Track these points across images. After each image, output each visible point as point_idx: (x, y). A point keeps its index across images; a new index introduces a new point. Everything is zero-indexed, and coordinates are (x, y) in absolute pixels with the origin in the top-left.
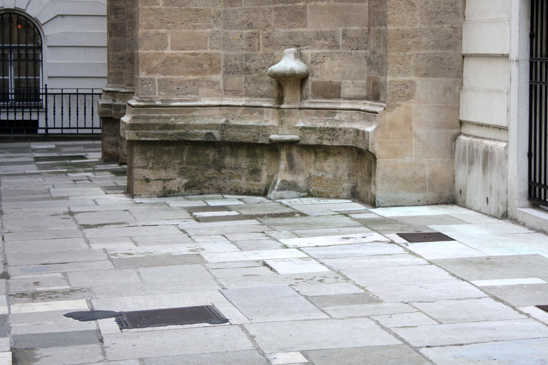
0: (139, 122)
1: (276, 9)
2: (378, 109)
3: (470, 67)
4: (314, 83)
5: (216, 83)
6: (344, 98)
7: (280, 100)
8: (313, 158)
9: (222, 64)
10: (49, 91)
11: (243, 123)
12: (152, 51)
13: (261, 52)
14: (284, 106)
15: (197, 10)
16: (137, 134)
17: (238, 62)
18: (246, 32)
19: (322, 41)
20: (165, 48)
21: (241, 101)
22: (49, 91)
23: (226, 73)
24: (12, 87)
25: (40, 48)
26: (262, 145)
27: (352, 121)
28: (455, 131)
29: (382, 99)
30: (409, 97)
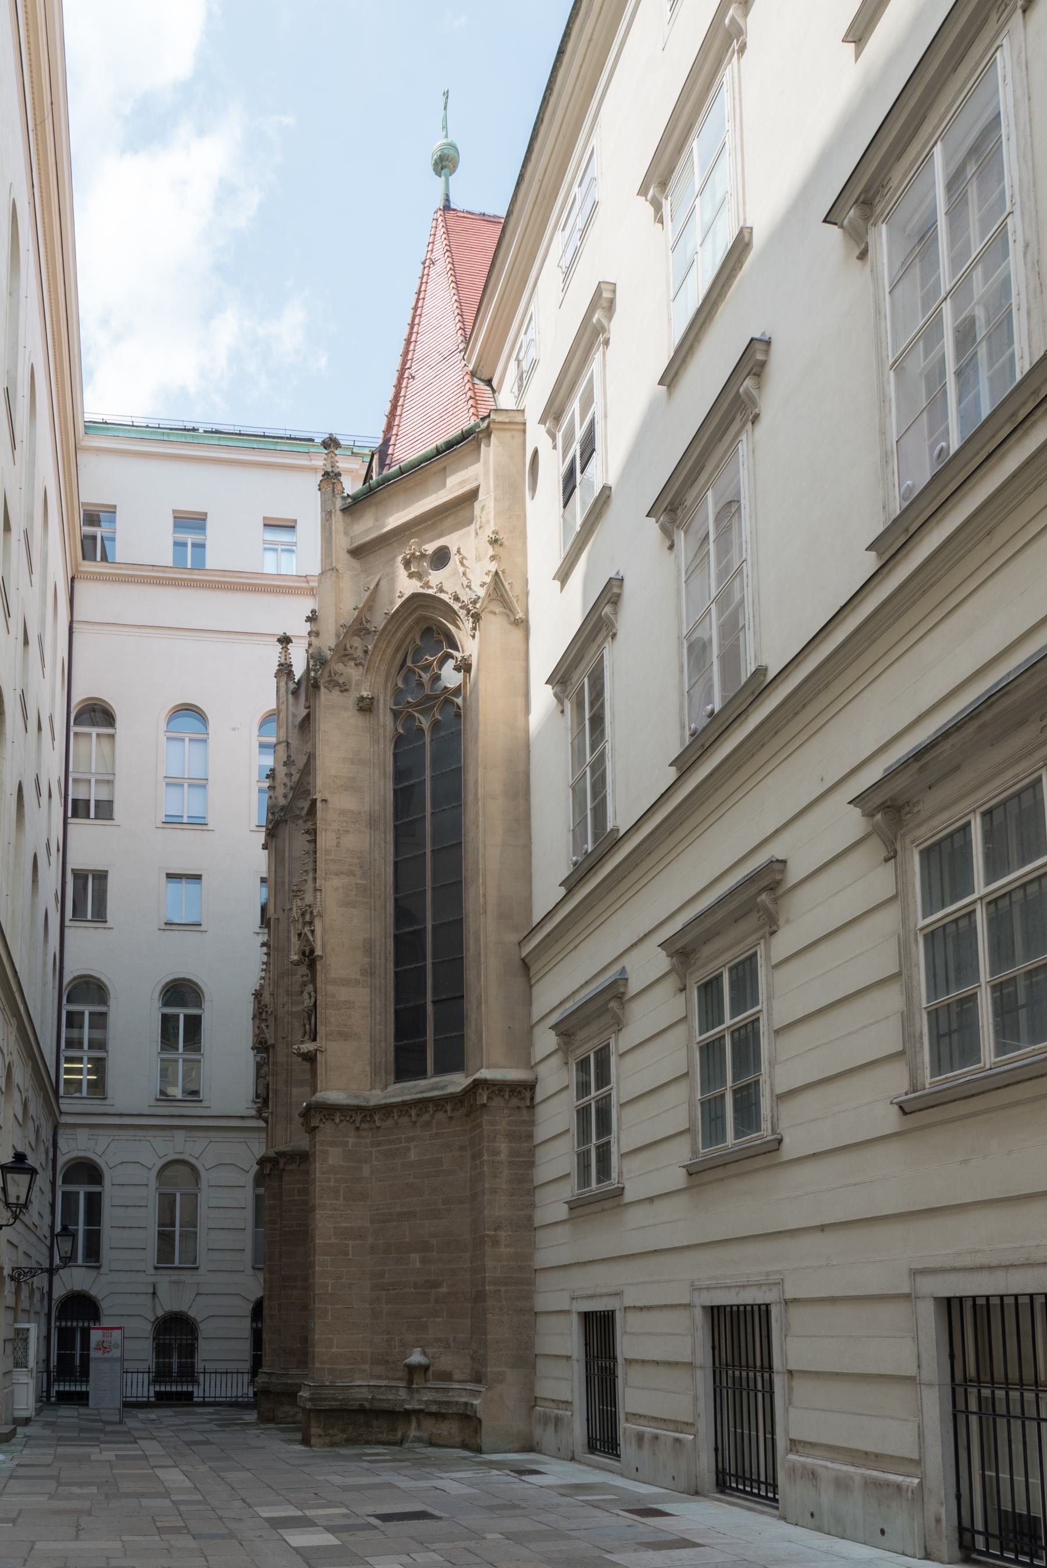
0: (315, 1396)
2: (483, 1390)
12: (324, 1350)
17: (380, 1357)
18: (386, 1337)
29: (483, 1382)
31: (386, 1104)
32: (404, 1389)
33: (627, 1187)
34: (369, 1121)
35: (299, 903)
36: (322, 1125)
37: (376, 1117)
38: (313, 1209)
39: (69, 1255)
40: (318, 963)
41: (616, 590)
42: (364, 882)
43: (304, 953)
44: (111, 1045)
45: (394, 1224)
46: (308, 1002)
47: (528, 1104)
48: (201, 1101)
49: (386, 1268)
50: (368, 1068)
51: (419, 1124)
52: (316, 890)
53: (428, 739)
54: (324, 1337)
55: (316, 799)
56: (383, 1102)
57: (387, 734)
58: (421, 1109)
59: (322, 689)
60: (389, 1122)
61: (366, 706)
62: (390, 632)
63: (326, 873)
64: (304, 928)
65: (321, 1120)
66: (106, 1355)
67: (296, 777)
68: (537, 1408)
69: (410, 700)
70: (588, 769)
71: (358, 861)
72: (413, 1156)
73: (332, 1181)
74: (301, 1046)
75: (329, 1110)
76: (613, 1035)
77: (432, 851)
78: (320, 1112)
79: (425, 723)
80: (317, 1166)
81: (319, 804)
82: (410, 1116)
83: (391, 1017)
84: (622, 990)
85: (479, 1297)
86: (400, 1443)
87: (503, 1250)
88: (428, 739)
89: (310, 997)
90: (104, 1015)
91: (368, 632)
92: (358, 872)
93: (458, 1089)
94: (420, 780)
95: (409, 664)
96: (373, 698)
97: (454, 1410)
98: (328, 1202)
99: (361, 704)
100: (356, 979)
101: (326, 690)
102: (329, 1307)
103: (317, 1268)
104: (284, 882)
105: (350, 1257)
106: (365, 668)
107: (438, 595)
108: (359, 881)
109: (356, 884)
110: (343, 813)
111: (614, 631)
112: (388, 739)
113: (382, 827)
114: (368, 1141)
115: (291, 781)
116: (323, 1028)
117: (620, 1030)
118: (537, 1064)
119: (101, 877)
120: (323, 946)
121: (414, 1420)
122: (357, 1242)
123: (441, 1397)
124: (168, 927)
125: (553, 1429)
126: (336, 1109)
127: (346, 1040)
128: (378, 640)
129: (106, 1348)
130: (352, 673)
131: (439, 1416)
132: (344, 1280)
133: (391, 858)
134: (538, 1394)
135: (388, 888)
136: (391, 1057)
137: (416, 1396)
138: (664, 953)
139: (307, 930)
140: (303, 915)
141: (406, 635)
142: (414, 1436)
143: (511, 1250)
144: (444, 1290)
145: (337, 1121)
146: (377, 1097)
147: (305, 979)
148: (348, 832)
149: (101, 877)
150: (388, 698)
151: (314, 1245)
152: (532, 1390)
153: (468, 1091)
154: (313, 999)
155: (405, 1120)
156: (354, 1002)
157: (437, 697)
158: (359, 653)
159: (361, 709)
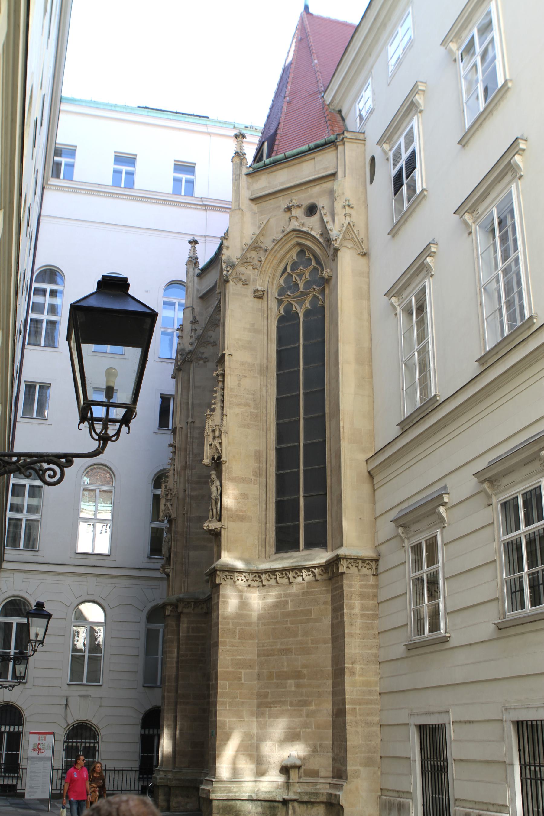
4: (304, 770)
6: (321, 777)
8: (305, 808)
30: (358, 777)
39: (23, 675)
40: (223, 465)
42: (256, 411)
43: (213, 458)
45: (275, 657)
49: (269, 691)
50: (256, 542)
52: (223, 415)
55: (225, 354)
59: (231, 283)
60: (273, 582)
61: (259, 295)
62: (276, 250)
63: (230, 404)
66: (41, 755)
69: (289, 293)
71: (251, 396)
73: (231, 625)
74: (210, 525)
78: (223, 573)
81: (227, 357)
83: (272, 507)
92: (252, 404)
95: (288, 270)
98: (227, 640)
99: (256, 294)
100: (250, 478)
105: (243, 681)
108: (252, 410)
109: (251, 412)
110: (242, 364)
112: (273, 317)
116: (226, 512)
120: (228, 454)
122: (248, 670)
127: (242, 521)
129: (40, 749)
132: (238, 699)
140: (213, 431)
148: (245, 376)
150: (274, 291)
153: (331, 563)
156: (247, 494)
158: (256, 262)
159: (256, 297)
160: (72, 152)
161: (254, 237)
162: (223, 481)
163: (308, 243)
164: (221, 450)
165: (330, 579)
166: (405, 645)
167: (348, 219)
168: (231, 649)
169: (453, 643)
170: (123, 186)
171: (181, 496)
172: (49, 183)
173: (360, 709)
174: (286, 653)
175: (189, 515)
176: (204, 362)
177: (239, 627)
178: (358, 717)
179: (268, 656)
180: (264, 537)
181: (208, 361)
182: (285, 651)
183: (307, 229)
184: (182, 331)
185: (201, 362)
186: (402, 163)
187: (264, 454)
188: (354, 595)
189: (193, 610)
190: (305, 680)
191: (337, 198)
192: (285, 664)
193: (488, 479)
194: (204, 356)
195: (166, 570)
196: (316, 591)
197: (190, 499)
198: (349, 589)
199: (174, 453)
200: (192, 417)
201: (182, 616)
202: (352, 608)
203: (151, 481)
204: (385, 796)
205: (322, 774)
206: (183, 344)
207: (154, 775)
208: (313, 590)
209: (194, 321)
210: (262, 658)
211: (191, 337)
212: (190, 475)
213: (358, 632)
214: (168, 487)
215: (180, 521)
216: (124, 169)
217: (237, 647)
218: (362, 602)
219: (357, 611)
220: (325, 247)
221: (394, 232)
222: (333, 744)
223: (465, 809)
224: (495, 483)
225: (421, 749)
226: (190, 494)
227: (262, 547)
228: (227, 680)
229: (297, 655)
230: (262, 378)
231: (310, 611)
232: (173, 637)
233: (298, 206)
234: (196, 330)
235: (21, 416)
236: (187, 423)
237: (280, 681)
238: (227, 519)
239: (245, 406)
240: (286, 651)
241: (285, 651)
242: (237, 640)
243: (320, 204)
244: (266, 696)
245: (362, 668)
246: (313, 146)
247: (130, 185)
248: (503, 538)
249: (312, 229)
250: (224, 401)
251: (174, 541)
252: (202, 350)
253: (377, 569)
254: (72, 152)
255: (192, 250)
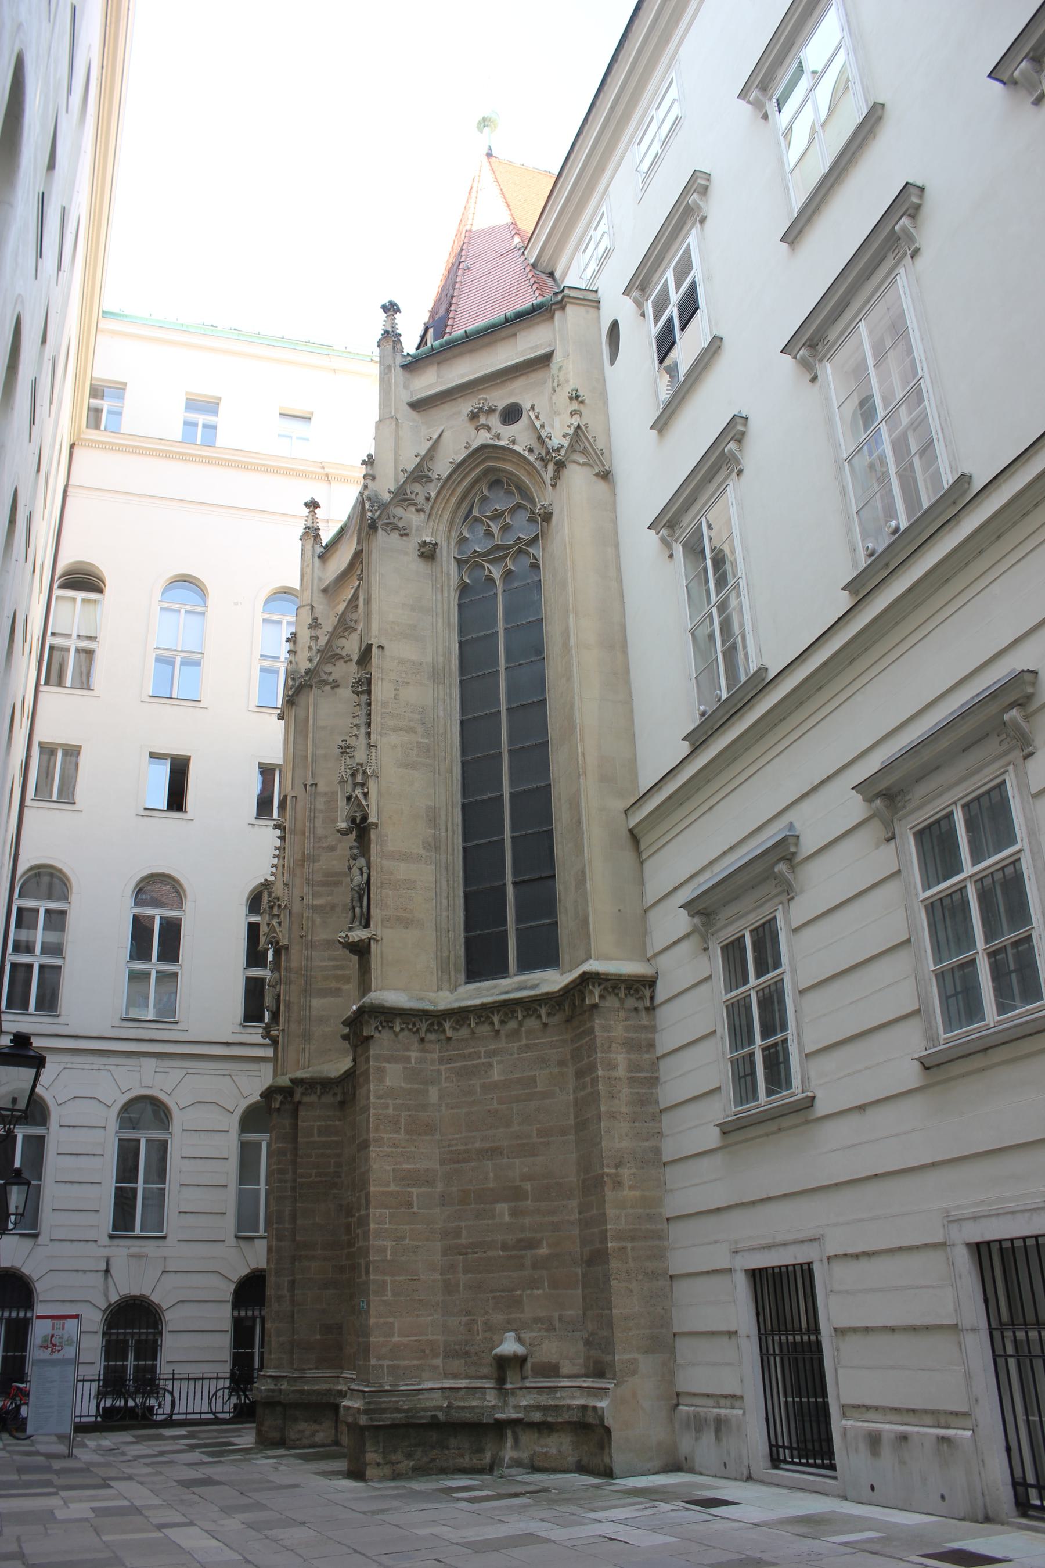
0: (372, 1406)
1: (494, 1298)
3: (681, 1344)
4: (533, 1364)
5: (436, 1367)
7: (501, 1380)
8: (536, 1435)
9: (442, 1348)
10: (176, 1376)
11: (466, 1404)
12: (382, 1339)
13: (480, 1337)
14: (509, 1386)
15: (420, 1300)
16: (371, 1419)
17: (457, 1347)
18: (464, 1319)
19: (539, 1325)
20: (393, 1336)
21: (463, 1383)
22: (176, 1376)
23: (445, 1357)
24: (130, 1371)
25: (161, 1333)
26: (487, 1425)
27: (573, 1397)
28: (675, 1402)
30: (634, 1373)
31: (460, 1008)
32: (493, 1392)
33: (819, 1095)
34: (436, 1031)
35: (349, 761)
36: (377, 1035)
37: (447, 1025)
38: (365, 1145)
40: (372, 831)
41: (740, 428)
42: (427, 741)
43: (353, 820)
44: (69, 950)
46: (358, 880)
47: (648, 1004)
48: (177, 1023)
49: (463, 1224)
50: (433, 964)
51: (502, 1033)
52: (370, 746)
53: (499, 590)
54: (382, 1321)
55: (371, 645)
56: (456, 1005)
57: (451, 583)
58: (506, 1014)
59: (380, 530)
60: (464, 1032)
61: (428, 553)
62: (455, 480)
63: (382, 728)
64: (354, 790)
65: (377, 1028)
67: (323, 641)
68: (681, 1407)
70: (715, 611)
71: (417, 717)
72: (496, 1074)
74: (350, 934)
75: (387, 1015)
76: (780, 907)
77: (508, 709)
78: (376, 1018)
79: (497, 573)
80: (372, 1087)
81: (374, 650)
82: (492, 1023)
84: (793, 849)
85: (597, 1257)
86: (490, 1469)
87: (626, 1193)
88: (499, 590)
89: (362, 874)
90: (63, 913)
91: (430, 480)
92: (420, 729)
93: (556, 987)
94: (490, 632)
95: (475, 513)
96: (436, 544)
97: (565, 1417)
99: (423, 550)
100: (418, 854)
101: (384, 532)
102: (388, 1279)
103: (372, 1226)
104: (306, 756)
105: (415, 1209)
106: (427, 514)
107: (511, 446)
109: (417, 742)
110: (402, 662)
111: (741, 466)
112: (452, 588)
113: (447, 681)
114: (435, 1056)
115: (316, 645)
116: (378, 911)
117: (792, 898)
118: (656, 955)
119: (72, 752)
121: (509, 1434)
122: (423, 1189)
123: (545, 1400)
124: (148, 813)
125: (713, 1437)
126: (396, 1015)
127: (406, 928)
128: (442, 487)
130: (412, 518)
131: (543, 1428)
132: (407, 1241)
133: (457, 717)
134: (682, 1387)
135: (454, 750)
136: (461, 950)
137: (512, 1401)
138: (860, 797)
139: (358, 792)
140: (353, 775)
141: (472, 486)
142: (511, 1459)
143: (637, 1193)
144: (543, 1251)
145: (397, 1029)
146: (445, 1000)
147: (356, 851)
149: (72, 752)
150: (452, 546)
151: (368, 1194)
152: (672, 1383)
154: (365, 876)
155: (484, 1029)
156: (415, 881)
157: (510, 547)
159: (422, 555)
160: (120, 388)
161: (418, 459)
162: (372, 859)
163: (509, 467)
164: (368, 805)
165: (569, 1020)
166: (718, 1125)
167: (575, 421)
168: (392, 1152)
169: (822, 1108)
170: (199, 442)
171: (296, 907)
172: (82, 436)
173: (633, 1248)
174: (492, 1155)
175: (310, 938)
176: (333, 688)
177: (407, 1113)
178: (631, 1264)
179: (459, 1162)
180: (445, 955)
181: (338, 686)
182: (489, 1153)
183: (507, 442)
184: (295, 642)
185: (328, 688)
186: (672, 310)
187: (443, 813)
188: (614, 1045)
189: (320, 1097)
190: (529, 1202)
191: (556, 388)
192: (491, 1175)
193: (884, 792)
194: (331, 679)
195: (272, 1033)
196: (543, 1043)
197: (311, 911)
198: (606, 1034)
199: (282, 838)
200: (313, 775)
201: (301, 1108)
202: (612, 1066)
203: (244, 902)
204: (687, 1405)
205: (564, 1370)
206: (296, 663)
207: (255, 1385)
208: (536, 1041)
209: (315, 625)
210: (448, 1167)
211: (310, 648)
212: (311, 871)
213: (624, 1109)
214: (273, 895)
215: (294, 951)
216: (201, 419)
217: (404, 1148)
218: (629, 1056)
219: (621, 1072)
220: (539, 468)
221: (662, 424)
222: (584, 1314)
223: (866, 1424)
224: (899, 798)
225: (758, 1314)
226: (310, 902)
227: (442, 972)
228: (386, 1207)
229: (513, 1158)
230: (436, 686)
231: (533, 1080)
232: (285, 1145)
233: (491, 411)
234: (317, 638)
235: (33, 797)
236: (305, 786)
237: (482, 1206)
238: (380, 924)
239: (407, 731)
240: (493, 1152)
241: (489, 1153)
242: (402, 1135)
243: (526, 406)
244: (457, 1233)
245: (634, 1174)
246: (512, 316)
247: (210, 442)
248: (923, 896)
249: (514, 442)
250: (372, 724)
251: (285, 984)
252: (328, 668)
253: (652, 998)
254: (120, 388)
255: (311, 517)
